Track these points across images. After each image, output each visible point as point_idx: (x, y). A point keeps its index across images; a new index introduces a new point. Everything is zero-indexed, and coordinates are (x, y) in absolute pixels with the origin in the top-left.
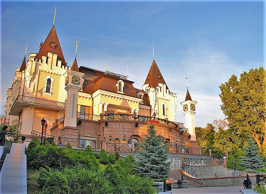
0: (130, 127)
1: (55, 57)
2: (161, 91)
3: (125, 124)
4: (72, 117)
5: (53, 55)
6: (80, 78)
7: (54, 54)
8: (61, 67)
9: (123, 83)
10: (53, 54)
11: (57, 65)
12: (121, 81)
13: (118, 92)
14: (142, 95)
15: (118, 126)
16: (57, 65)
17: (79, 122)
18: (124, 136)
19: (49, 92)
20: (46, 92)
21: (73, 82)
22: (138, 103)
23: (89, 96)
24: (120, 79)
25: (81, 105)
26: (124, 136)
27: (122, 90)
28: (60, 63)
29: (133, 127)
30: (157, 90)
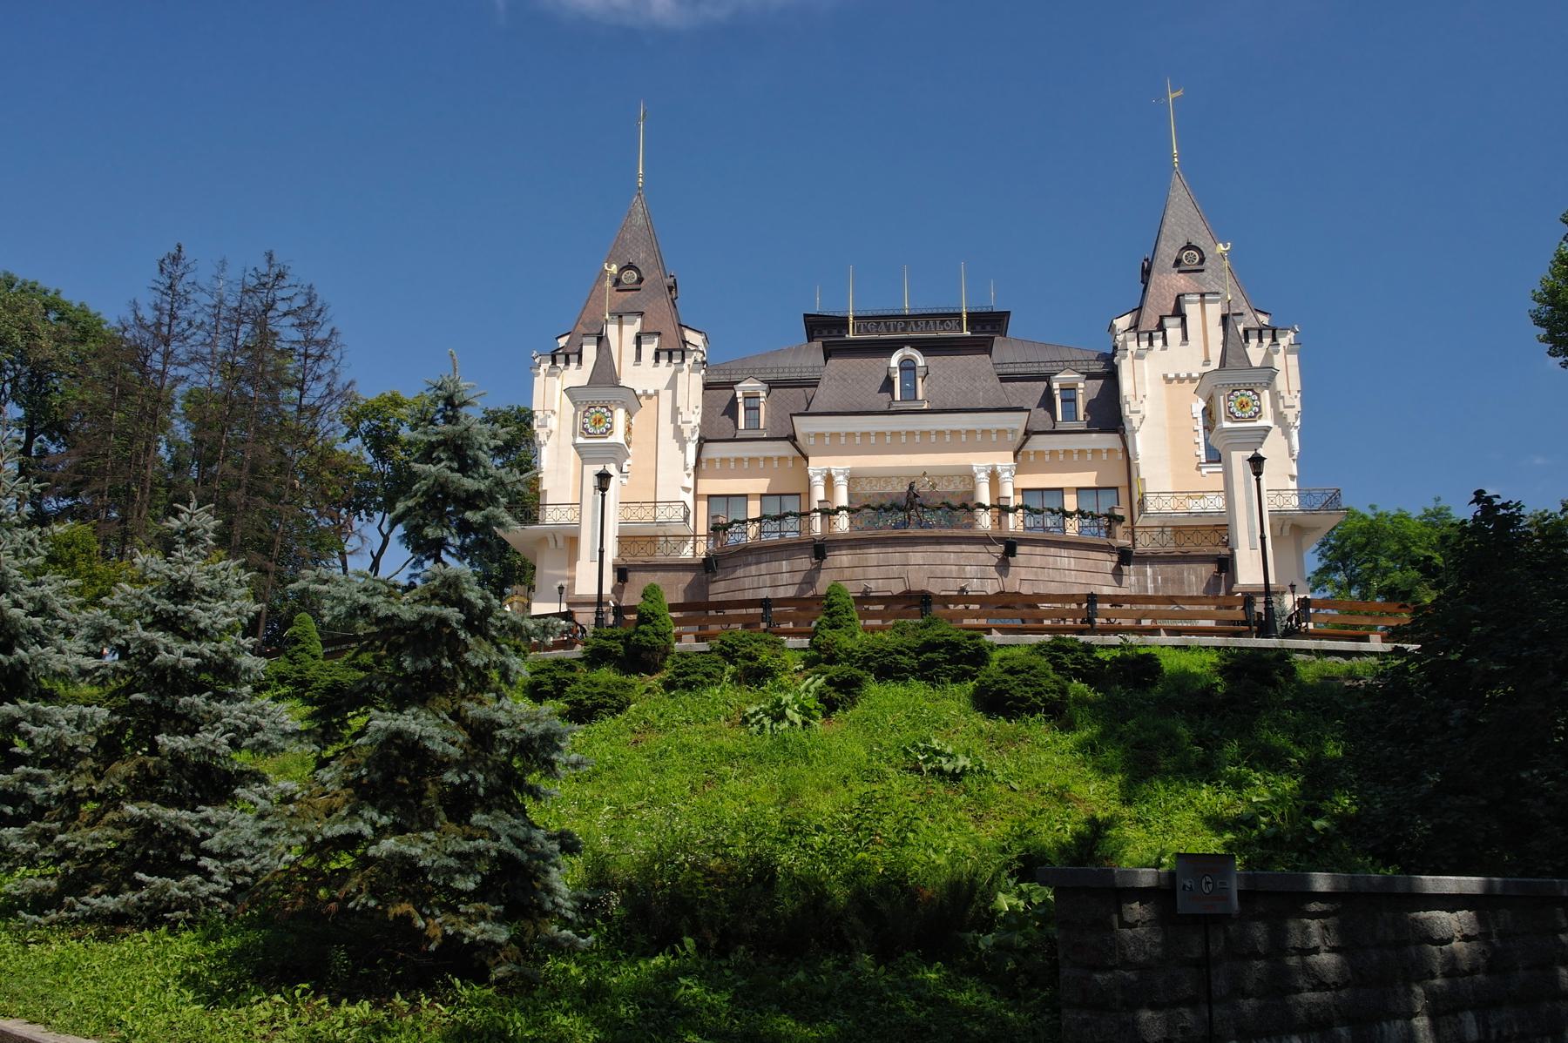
2: (1185, 337)
8: (657, 360)
9: (920, 361)
11: (639, 357)
16: (639, 357)
30: (1158, 343)
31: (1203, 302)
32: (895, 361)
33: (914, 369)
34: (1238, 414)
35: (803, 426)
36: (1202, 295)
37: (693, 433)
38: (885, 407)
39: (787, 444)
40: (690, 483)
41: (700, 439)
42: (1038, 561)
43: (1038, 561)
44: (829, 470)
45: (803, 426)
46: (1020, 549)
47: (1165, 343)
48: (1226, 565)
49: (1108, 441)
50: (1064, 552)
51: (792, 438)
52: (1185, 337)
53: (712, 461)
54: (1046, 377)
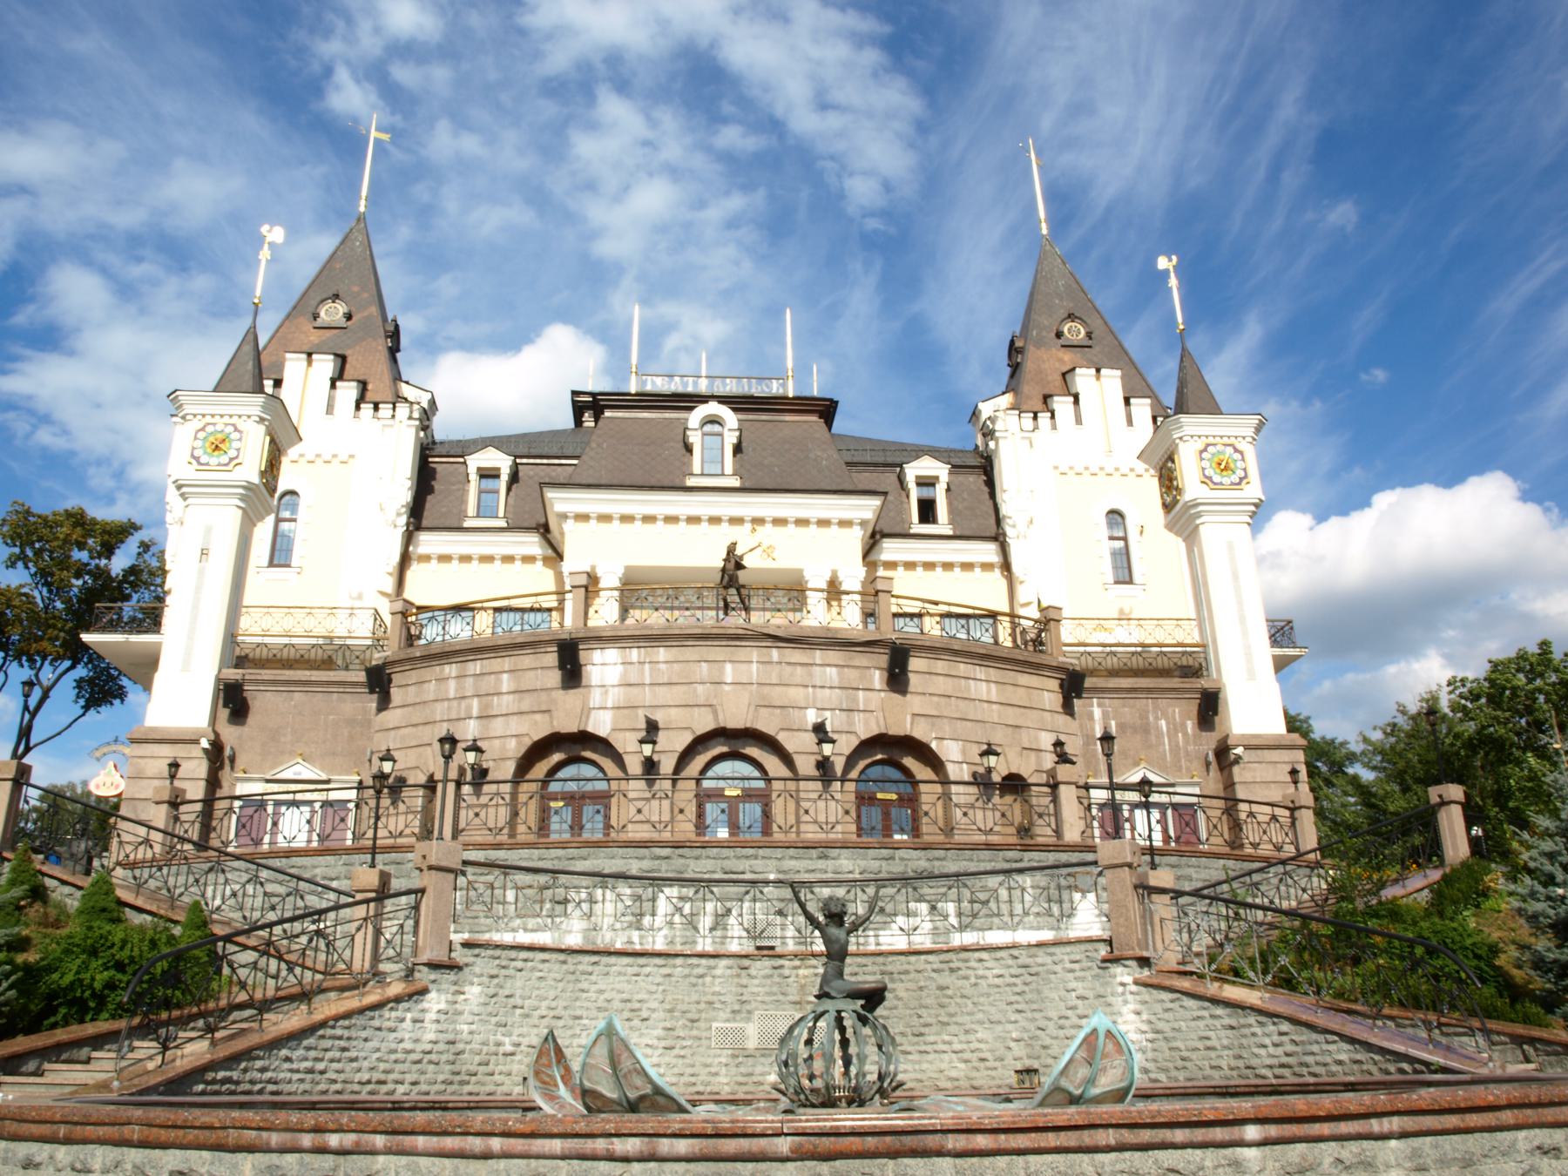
1: (325, 365)
2: (1079, 421)
5: (310, 362)
10: (310, 355)
11: (330, 409)
12: (713, 408)
13: (690, 482)
14: (937, 478)
15: (452, 684)
16: (330, 409)
19: (289, 566)
20: (271, 564)
21: (197, 459)
24: (703, 399)
28: (348, 391)
29: (555, 677)
33: (721, 435)
34: (1217, 479)
35: (561, 502)
36: (1098, 371)
37: (399, 515)
38: (677, 483)
40: (389, 585)
41: (408, 524)
42: (942, 685)
43: (942, 685)
45: (561, 502)
46: (915, 663)
48: (1209, 706)
49: (987, 552)
50: (980, 672)
51: (544, 530)
52: (1079, 421)
53: (426, 558)
54: (896, 467)
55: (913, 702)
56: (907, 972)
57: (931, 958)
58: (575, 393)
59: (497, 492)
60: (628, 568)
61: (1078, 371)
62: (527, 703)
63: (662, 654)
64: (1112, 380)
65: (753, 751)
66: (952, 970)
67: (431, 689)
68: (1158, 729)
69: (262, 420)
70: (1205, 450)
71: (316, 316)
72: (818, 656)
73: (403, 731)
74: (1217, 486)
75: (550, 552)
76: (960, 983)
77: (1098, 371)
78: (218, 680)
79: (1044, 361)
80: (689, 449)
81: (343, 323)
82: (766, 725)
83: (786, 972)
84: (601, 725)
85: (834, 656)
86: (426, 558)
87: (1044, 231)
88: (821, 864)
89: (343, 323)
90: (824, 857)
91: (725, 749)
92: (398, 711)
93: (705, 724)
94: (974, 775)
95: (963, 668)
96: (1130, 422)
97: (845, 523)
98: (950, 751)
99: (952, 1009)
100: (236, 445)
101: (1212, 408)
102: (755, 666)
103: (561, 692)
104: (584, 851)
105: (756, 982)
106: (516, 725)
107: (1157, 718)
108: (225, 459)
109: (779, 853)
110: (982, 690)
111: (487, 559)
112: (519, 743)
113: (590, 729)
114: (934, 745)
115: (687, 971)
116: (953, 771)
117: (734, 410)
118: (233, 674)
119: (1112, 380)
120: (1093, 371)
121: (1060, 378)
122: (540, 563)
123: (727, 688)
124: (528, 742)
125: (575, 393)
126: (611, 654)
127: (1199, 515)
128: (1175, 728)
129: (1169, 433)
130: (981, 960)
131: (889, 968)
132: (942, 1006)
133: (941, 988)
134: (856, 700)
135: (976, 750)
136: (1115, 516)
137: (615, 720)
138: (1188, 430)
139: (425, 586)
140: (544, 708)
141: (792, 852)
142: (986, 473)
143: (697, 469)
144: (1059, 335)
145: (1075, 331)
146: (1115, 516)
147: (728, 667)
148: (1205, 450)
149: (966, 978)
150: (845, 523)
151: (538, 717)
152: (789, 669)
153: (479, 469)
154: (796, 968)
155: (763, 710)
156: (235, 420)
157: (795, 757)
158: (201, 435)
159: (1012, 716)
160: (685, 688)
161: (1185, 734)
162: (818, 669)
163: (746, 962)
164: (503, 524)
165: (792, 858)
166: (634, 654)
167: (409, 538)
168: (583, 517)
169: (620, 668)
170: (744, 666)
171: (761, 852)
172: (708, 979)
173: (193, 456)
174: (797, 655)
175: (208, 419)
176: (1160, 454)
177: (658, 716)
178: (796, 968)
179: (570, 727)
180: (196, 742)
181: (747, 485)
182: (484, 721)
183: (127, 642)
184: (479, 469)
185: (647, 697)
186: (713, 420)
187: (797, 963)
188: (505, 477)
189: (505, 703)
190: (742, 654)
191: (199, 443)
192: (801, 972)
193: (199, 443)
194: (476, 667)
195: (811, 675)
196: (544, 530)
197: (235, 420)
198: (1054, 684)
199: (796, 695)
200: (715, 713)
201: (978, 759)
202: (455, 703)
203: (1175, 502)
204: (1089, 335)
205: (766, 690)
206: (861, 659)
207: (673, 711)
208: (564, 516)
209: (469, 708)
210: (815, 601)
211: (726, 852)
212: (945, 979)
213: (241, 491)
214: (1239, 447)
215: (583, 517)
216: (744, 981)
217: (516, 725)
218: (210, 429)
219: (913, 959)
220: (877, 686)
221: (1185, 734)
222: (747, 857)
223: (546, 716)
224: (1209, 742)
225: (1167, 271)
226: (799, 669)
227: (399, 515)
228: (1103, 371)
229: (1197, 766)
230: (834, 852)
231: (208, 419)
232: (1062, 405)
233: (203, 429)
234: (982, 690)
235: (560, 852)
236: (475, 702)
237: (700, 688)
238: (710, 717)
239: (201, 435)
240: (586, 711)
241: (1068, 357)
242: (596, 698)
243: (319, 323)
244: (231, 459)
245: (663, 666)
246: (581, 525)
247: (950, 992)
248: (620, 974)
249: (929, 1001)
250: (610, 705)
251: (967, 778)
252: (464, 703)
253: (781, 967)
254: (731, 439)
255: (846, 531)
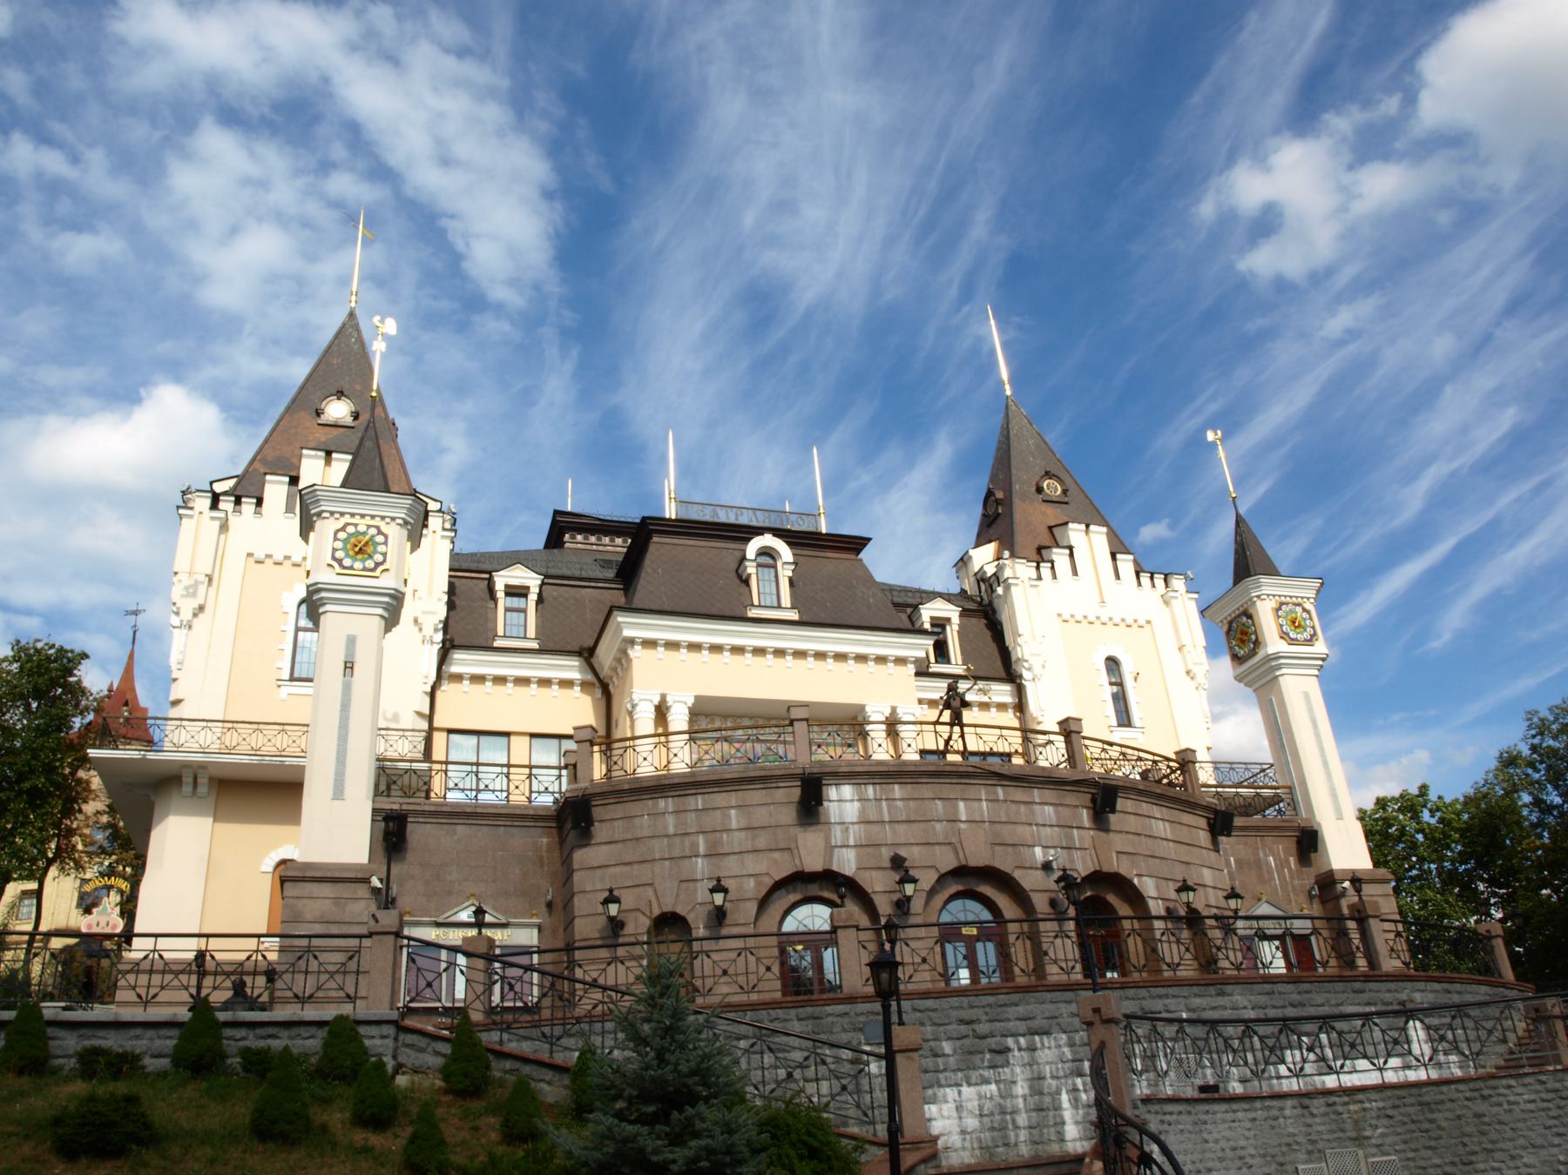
0: (761, 816)
2: (1075, 573)
3: (720, 799)
4: (338, 793)
6: (384, 529)
7: (334, 455)
12: (768, 540)
13: (753, 613)
14: (948, 620)
15: (670, 821)
17: (392, 832)
18: (712, 891)
21: (340, 562)
22: (911, 669)
23: (571, 668)
24: (760, 531)
25: (533, 735)
26: (712, 891)
27: (786, 600)
29: (788, 815)
31: (1087, 531)
32: (752, 548)
34: (1292, 635)
36: (1087, 526)
37: (436, 630)
38: (738, 614)
39: (575, 662)
41: (444, 642)
44: (663, 697)
46: (1121, 804)
47: (1055, 577)
48: (1308, 841)
50: (1157, 811)
52: (1075, 573)
53: (458, 678)
55: (1118, 842)
56: (1442, 1102)
57: (1461, 1087)
58: (556, 513)
59: (524, 611)
60: (697, 698)
61: (1071, 525)
62: (762, 841)
63: (897, 791)
64: (1099, 534)
65: (987, 890)
66: (1484, 1098)
67: (644, 825)
68: (1268, 864)
69: (406, 523)
70: (1279, 609)
71: (318, 413)
72: (1036, 795)
73: (612, 870)
74: (1293, 642)
75: (590, 677)
76: (1495, 1109)
77: (1087, 526)
78: (374, 810)
79: (1029, 515)
80: (746, 582)
81: (349, 420)
82: (1004, 863)
83: (1340, 1109)
84: (846, 862)
85: (1050, 795)
86: (458, 678)
87: (1008, 393)
88: (1221, 1001)
89: (349, 420)
90: (1222, 994)
91: (960, 888)
92: (605, 848)
93: (948, 862)
94: (1168, 910)
95: (1145, 808)
96: (1118, 577)
97: (901, 661)
98: (1148, 887)
99: (1493, 1136)
100: (382, 548)
101: (1272, 571)
102: (984, 804)
103: (798, 829)
104: (1015, 997)
105: (1317, 1120)
106: (754, 865)
107: (1266, 856)
108: (370, 564)
109: (1185, 991)
110: (1161, 829)
111: (523, 681)
112: (758, 884)
113: (835, 868)
114: (1136, 881)
115: (1266, 1113)
116: (1157, 908)
117: (789, 544)
118: (393, 804)
119: (1099, 534)
120: (1083, 527)
121: (1046, 531)
122: (578, 689)
123: (963, 826)
124: (769, 882)
125: (556, 513)
126: (847, 791)
127: (1279, 667)
128: (1282, 864)
129: (1248, 591)
130: (1509, 1087)
131: (1426, 1099)
132: (1483, 1133)
133: (1478, 1116)
134: (1071, 838)
135: (1172, 886)
136: (1113, 664)
137: (859, 858)
138: (1266, 590)
139: (459, 705)
140: (782, 845)
141: (1195, 989)
142: (986, 616)
143: (756, 602)
144: (1039, 490)
145: (1052, 488)
146: (1113, 664)
147: (961, 804)
148: (1279, 609)
149: (1500, 1105)
150: (901, 661)
151: (777, 855)
152: (1013, 807)
153: (507, 586)
154: (1346, 1104)
155: (997, 848)
156: (377, 522)
157: (1032, 894)
158: (342, 535)
159: (1182, 853)
160: (923, 825)
161: (1290, 869)
162: (1037, 807)
163: (1306, 1101)
164: (535, 645)
165: (1196, 995)
166: (870, 791)
167: (443, 658)
168: (650, 644)
169: (857, 805)
170: (975, 805)
171: (1171, 991)
172: (1281, 1120)
173: (334, 558)
174: (1019, 794)
175: (347, 519)
176: (1230, 610)
177: (903, 852)
178: (1346, 1104)
179: (814, 864)
180: (367, 881)
181: (805, 619)
182: (715, 860)
183: (144, 759)
184: (507, 586)
185: (888, 833)
186: (766, 552)
187: (1346, 1099)
188: (533, 597)
189: (738, 840)
190: (971, 792)
191: (339, 545)
192: (1352, 1107)
193: (339, 545)
194: (699, 802)
195: (1032, 813)
196: (587, 654)
197: (377, 522)
198: (1203, 823)
199: (1024, 832)
200: (955, 850)
201: (1173, 895)
202: (677, 840)
203: (1253, 653)
204: (1065, 492)
205: (998, 827)
206: (1071, 799)
207: (915, 849)
208: (631, 642)
209: (695, 845)
210: (877, 733)
211: (1143, 992)
212: (1481, 1107)
213: (386, 599)
214: (1308, 606)
215: (650, 644)
216: (1309, 1120)
217: (754, 865)
218: (351, 529)
219: (1444, 1088)
220: (1087, 824)
221: (1290, 869)
222: (1160, 997)
223: (786, 853)
224: (1308, 879)
225: (1214, 444)
226: (1023, 808)
227: (436, 630)
228: (1092, 527)
229: (1303, 899)
230: (1229, 988)
231: (347, 519)
232: (1060, 557)
233: (343, 529)
234: (1161, 829)
235: (991, 999)
236: (701, 839)
237: (938, 826)
238: (952, 856)
239: (342, 535)
240: (830, 849)
241: (1052, 515)
242: (837, 835)
243: (324, 419)
244: (377, 565)
245: (899, 804)
246: (649, 653)
247: (1487, 1119)
248: (1224, 1121)
249: (1468, 1129)
250: (852, 843)
251: (1163, 913)
252: (687, 841)
253: (1334, 1104)
254: (785, 573)
255: (901, 669)
